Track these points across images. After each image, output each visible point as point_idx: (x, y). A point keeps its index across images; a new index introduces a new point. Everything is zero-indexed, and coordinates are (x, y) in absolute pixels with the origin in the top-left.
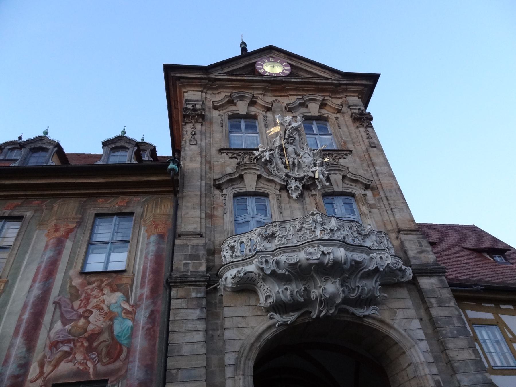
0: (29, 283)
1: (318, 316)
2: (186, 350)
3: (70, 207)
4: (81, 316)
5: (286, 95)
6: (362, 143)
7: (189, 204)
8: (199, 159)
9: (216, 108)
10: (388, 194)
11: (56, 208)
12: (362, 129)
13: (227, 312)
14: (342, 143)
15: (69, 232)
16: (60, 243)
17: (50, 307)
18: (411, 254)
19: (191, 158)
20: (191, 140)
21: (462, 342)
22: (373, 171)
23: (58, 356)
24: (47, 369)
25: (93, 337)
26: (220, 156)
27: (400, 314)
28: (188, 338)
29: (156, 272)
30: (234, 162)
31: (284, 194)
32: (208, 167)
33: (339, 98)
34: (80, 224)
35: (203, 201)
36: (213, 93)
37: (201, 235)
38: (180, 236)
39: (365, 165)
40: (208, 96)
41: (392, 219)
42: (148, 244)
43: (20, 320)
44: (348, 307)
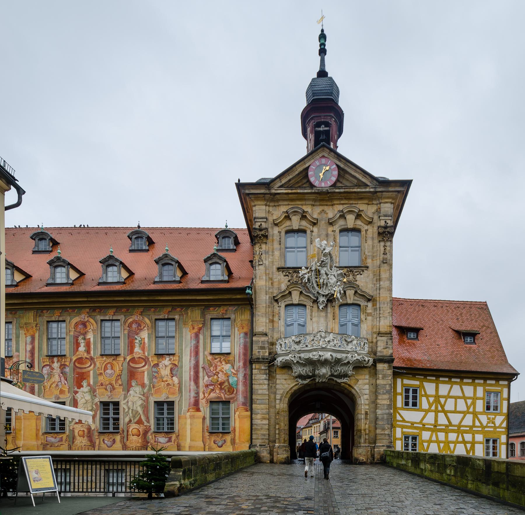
0: (189, 357)
1: (318, 382)
2: (260, 392)
3: (196, 314)
4: (215, 374)
5: (330, 204)
6: (378, 258)
7: (259, 313)
8: (264, 278)
9: (276, 225)
10: (382, 306)
11: (189, 314)
12: (382, 244)
13: (278, 376)
14: (364, 258)
15: (200, 329)
16: (197, 336)
17: (201, 370)
18: (379, 349)
19: (260, 277)
20: (259, 261)
21: (386, 396)
22: (378, 285)
23: (209, 390)
24: (206, 395)
25: (221, 384)
26: (278, 273)
27: (360, 382)
28: (261, 387)
29: (245, 354)
30: (287, 279)
31: (315, 306)
32: (270, 284)
33: (375, 204)
34: (204, 324)
35: (267, 311)
36: (275, 206)
37: (266, 335)
38: (255, 335)
39: (375, 279)
40: (271, 209)
41: (378, 324)
42: (240, 338)
43: (190, 375)
44: (334, 378)
